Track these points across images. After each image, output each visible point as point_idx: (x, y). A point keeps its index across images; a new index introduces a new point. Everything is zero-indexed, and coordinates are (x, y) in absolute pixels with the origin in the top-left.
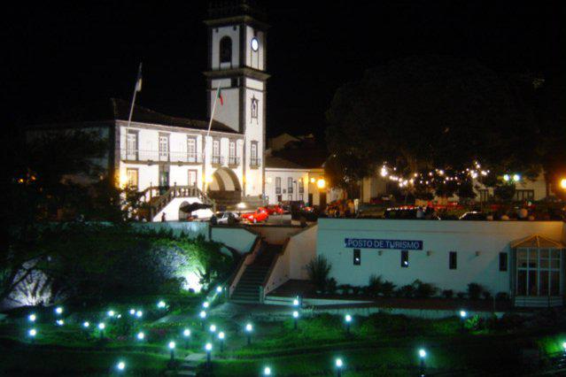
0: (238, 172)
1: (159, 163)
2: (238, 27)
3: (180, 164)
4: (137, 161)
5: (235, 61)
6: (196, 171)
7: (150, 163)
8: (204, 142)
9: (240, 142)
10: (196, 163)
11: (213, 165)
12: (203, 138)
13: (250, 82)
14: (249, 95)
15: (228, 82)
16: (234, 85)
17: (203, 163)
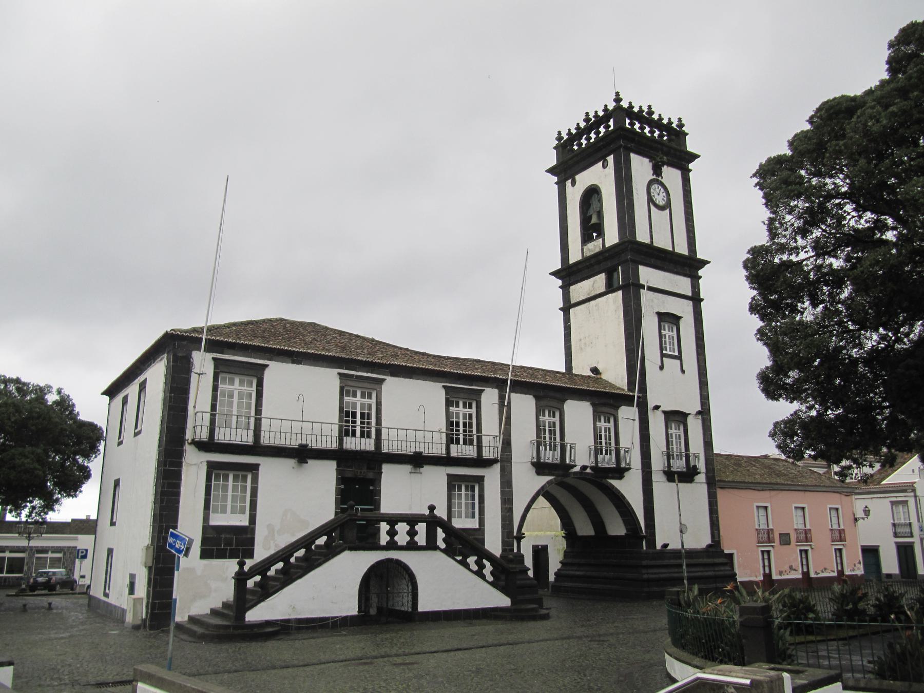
0: (630, 488)
1: (340, 456)
2: (611, 159)
3: (417, 461)
4: (257, 449)
5: (612, 236)
6: (480, 480)
7: (303, 454)
8: (504, 406)
9: (628, 415)
10: (481, 462)
11: (540, 468)
12: (502, 398)
13: (647, 275)
14: (650, 305)
15: (599, 282)
16: (610, 288)
17: (505, 460)
